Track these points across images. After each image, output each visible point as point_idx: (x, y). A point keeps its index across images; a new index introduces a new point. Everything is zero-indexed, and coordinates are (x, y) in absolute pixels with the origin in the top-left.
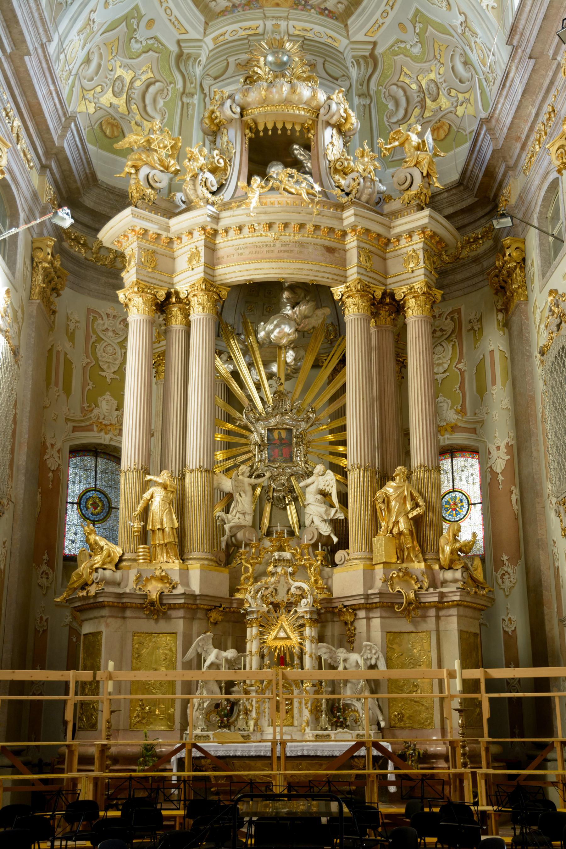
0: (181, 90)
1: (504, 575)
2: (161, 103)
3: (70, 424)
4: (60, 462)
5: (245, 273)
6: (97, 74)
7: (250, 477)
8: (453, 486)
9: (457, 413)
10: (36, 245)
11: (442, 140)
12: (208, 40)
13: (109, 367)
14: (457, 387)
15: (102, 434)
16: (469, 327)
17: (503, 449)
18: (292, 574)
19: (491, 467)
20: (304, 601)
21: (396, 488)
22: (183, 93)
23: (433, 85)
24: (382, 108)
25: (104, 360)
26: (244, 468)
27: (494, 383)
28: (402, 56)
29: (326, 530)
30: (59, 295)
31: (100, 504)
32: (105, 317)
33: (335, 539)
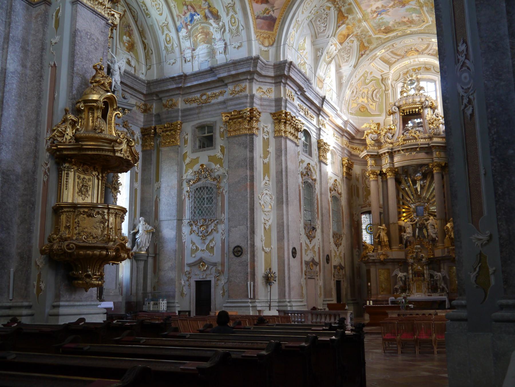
2: (378, 96)
3: (360, 207)
6: (356, 94)
10: (343, 160)
12: (392, 71)
18: (420, 252)
30: (352, 170)
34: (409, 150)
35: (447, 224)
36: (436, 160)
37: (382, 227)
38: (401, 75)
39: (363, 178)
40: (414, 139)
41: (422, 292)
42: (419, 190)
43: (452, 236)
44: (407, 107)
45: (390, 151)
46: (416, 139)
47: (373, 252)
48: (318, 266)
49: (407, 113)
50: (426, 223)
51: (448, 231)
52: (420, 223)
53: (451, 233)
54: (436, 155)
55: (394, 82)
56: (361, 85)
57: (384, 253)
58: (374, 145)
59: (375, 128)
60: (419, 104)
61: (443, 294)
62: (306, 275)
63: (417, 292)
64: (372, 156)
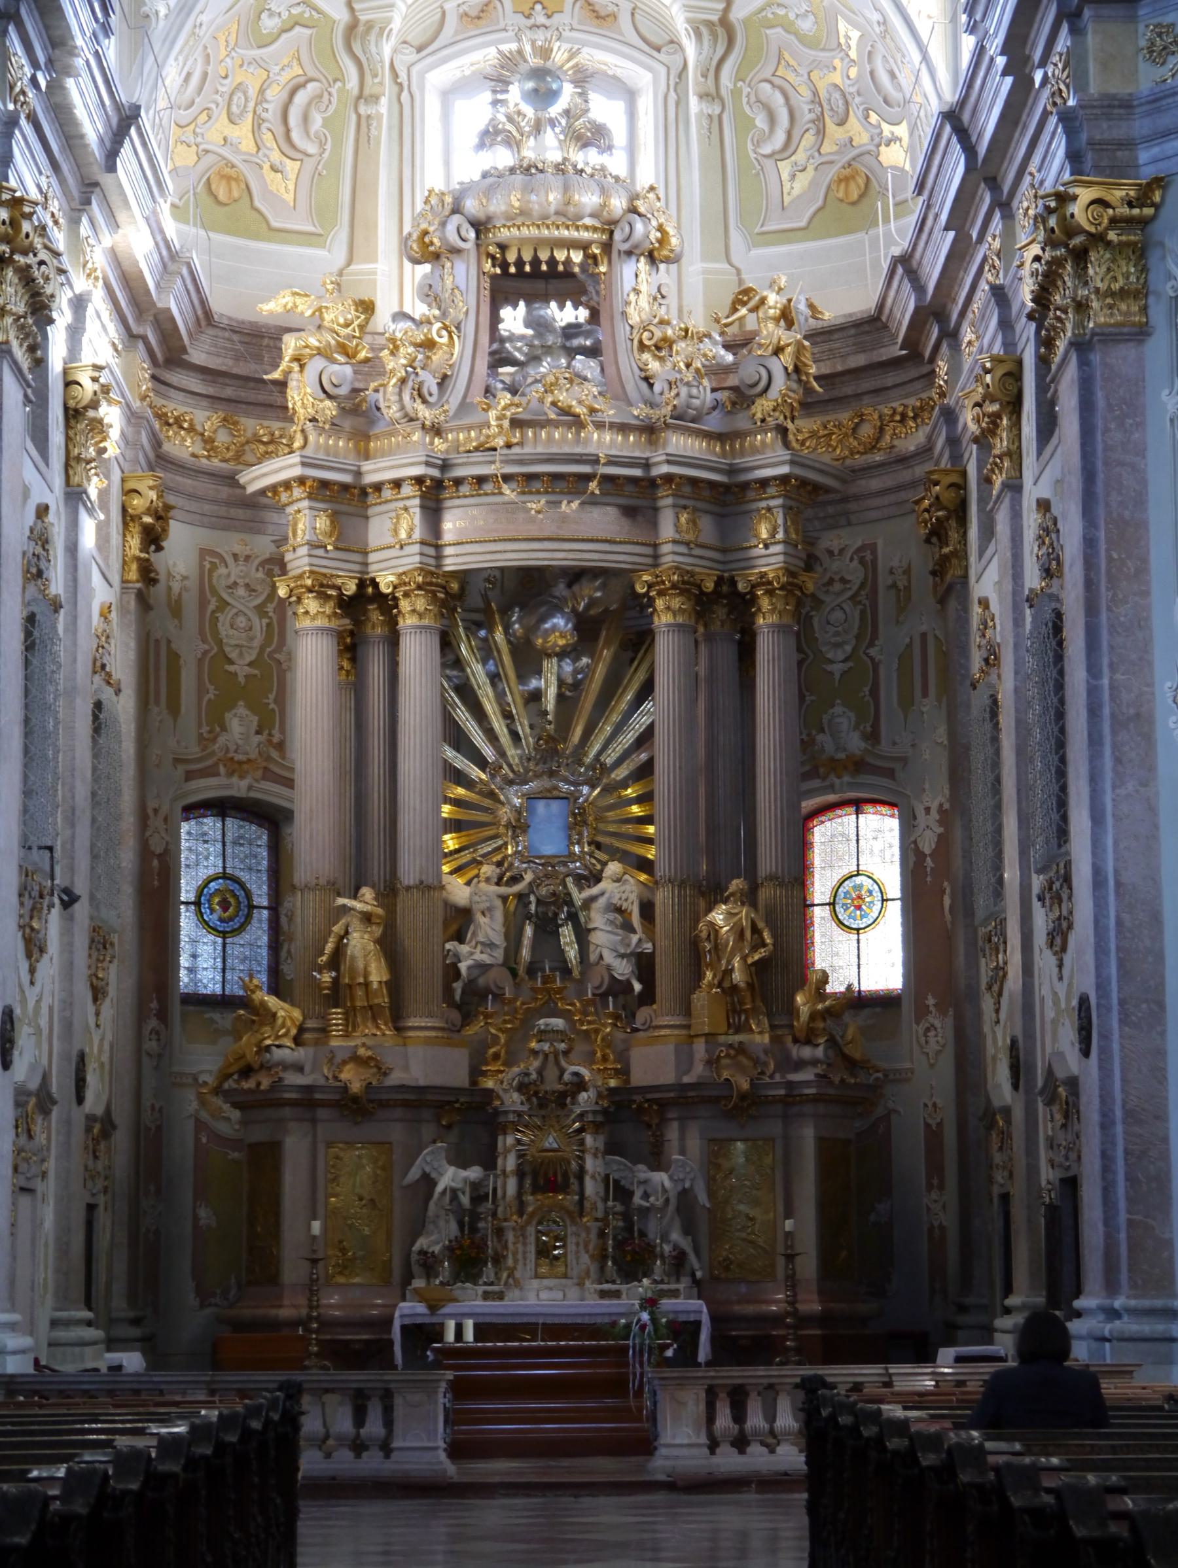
0: (356, 92)
1: (928, 1030)
2: (317, 121)
3: (181, 769)
4: (168, 838)
5: (489, 557)
7: (498, 884)
8: (858, 865)
9: (866, 737)
10: (131, 485)
11: (853, 204)
13: (241, 654)
14: (866, 689)
15: (235, 779)
16: (890, 582)
17: (934, 815)
18: (566, 1053)
19: (915, 842)
20: (583, 1096)
21: (730, 915)
22: (360, 97)
23: (837, 95)
24: (744, 124)
25: (233, 642)
26: (487, 870)
27: (925, 694)
28: (779, 30)
29: (623, 969)
31: (232, 900)
32: (230, 560)
33: (637, 987)
34: (537, 485)
35: (709, 910)
36: (670, 555)
37: (358, 906)
38: (451, 23)
39: (203, 603)
40: (569, 426)
41: (565, 1276)
42: (550, 701)
43: (738, 977)
44: (525, 231)
45: (436, 473)
46: (577, 423)
47: (298, 1041)
49: (520, 263)
50: (578, 897)
51: (717, 949)
52: (543, 891)
53: (729, 962)
54: (678, 531)
55: (410, 56)
56: (232, 43)
57: (362, 1052)
58: (335, 426)
59: (347, 325)
60: (595, 229)
61: (681, 1286)
63: (537, 1276)
64: (322, 490)
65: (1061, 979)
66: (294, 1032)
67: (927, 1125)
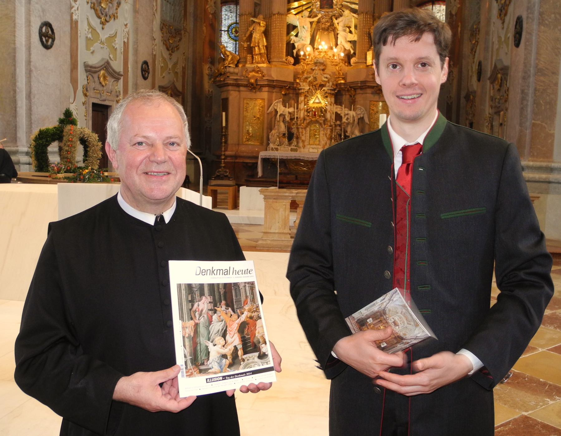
48: (121, 81)
62: (85, 95)
65: (503, 28)
66: (236, 63)
67: (448, 103)
